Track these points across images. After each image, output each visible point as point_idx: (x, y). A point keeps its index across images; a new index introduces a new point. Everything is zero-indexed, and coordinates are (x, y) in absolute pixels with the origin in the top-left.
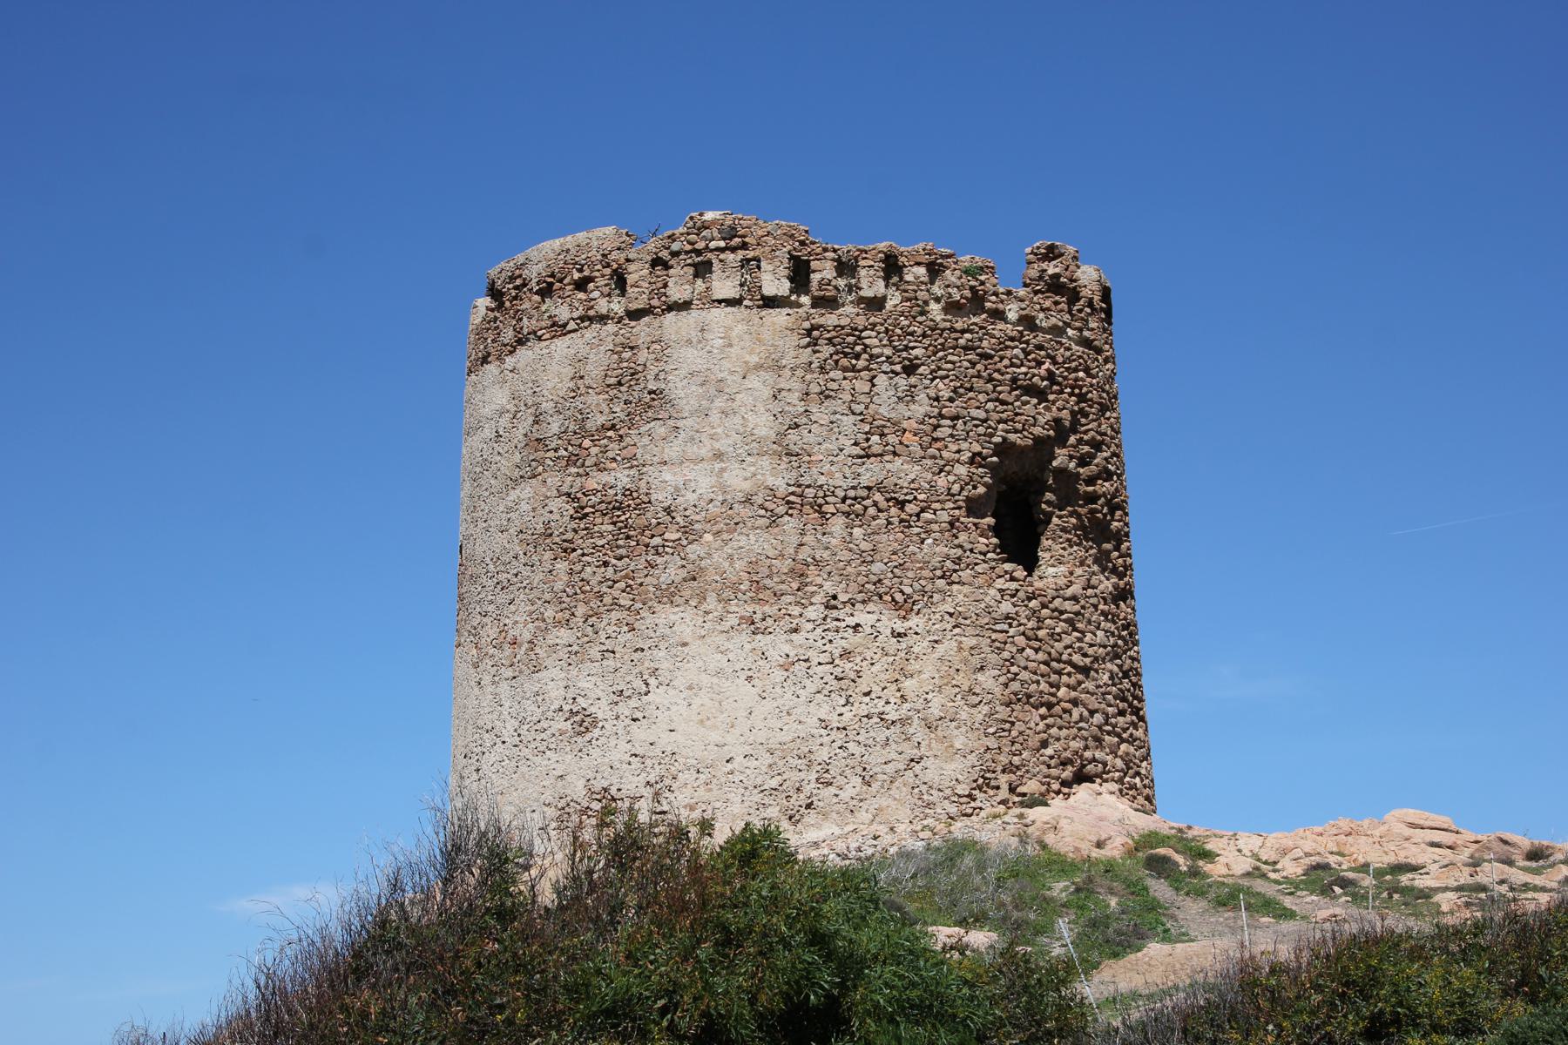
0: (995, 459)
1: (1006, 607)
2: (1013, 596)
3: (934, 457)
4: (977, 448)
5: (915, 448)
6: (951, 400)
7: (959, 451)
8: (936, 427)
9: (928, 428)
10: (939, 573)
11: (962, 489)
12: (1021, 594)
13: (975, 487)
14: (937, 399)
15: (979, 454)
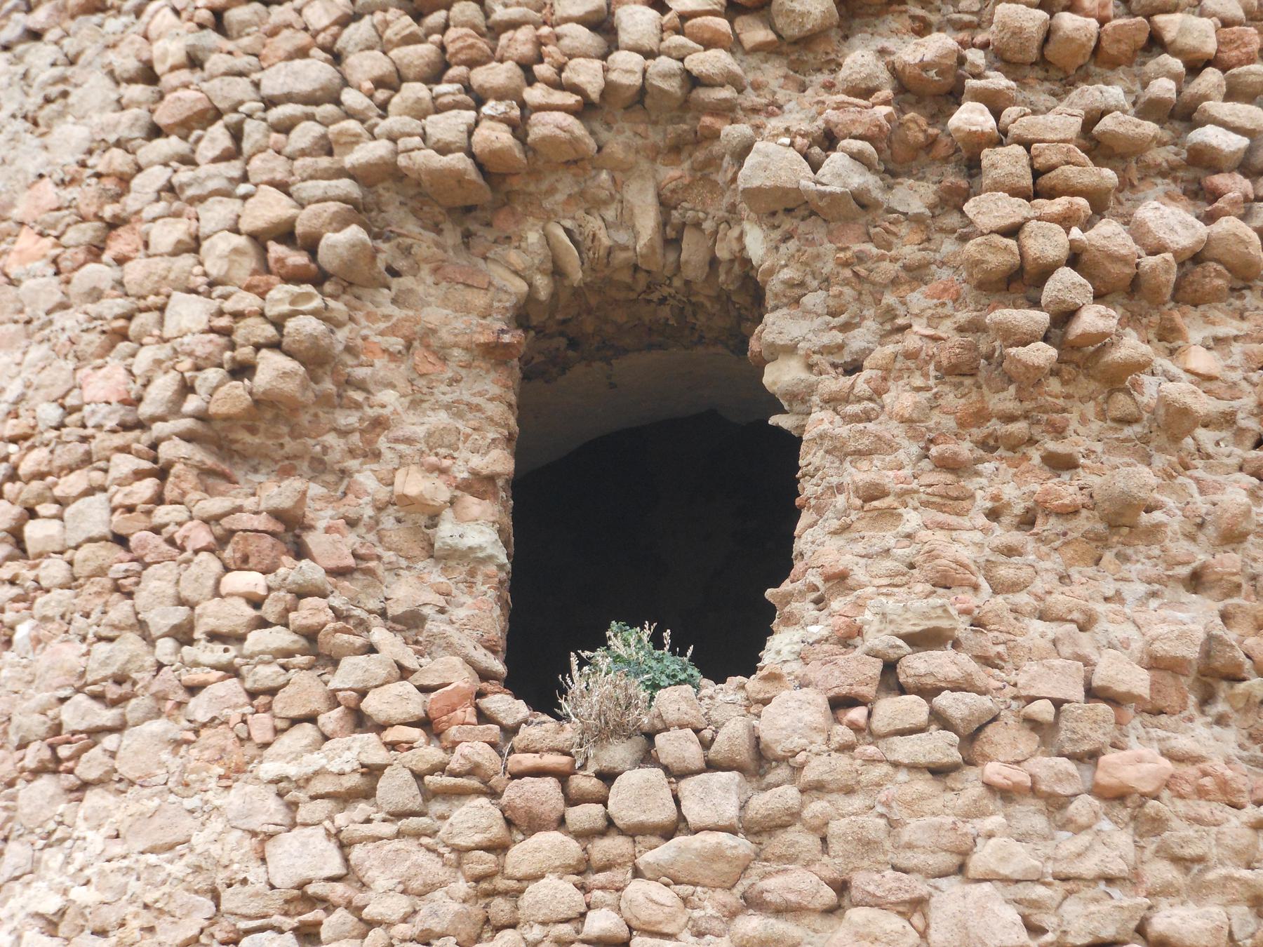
0: (354, 233)
1: (305, 855)
2: (345, 798)
3: (95, 295)
4: (269, 208)
5: (40, 288)
6: (194, 61)
7: (194, 245)
8: (124, 180)
9: (85, 195)
10: (36, 753)
11: (187, 388)
12: (396, 788)
13: (242, 370)
14: (148, 75)
15: (285, 234)
